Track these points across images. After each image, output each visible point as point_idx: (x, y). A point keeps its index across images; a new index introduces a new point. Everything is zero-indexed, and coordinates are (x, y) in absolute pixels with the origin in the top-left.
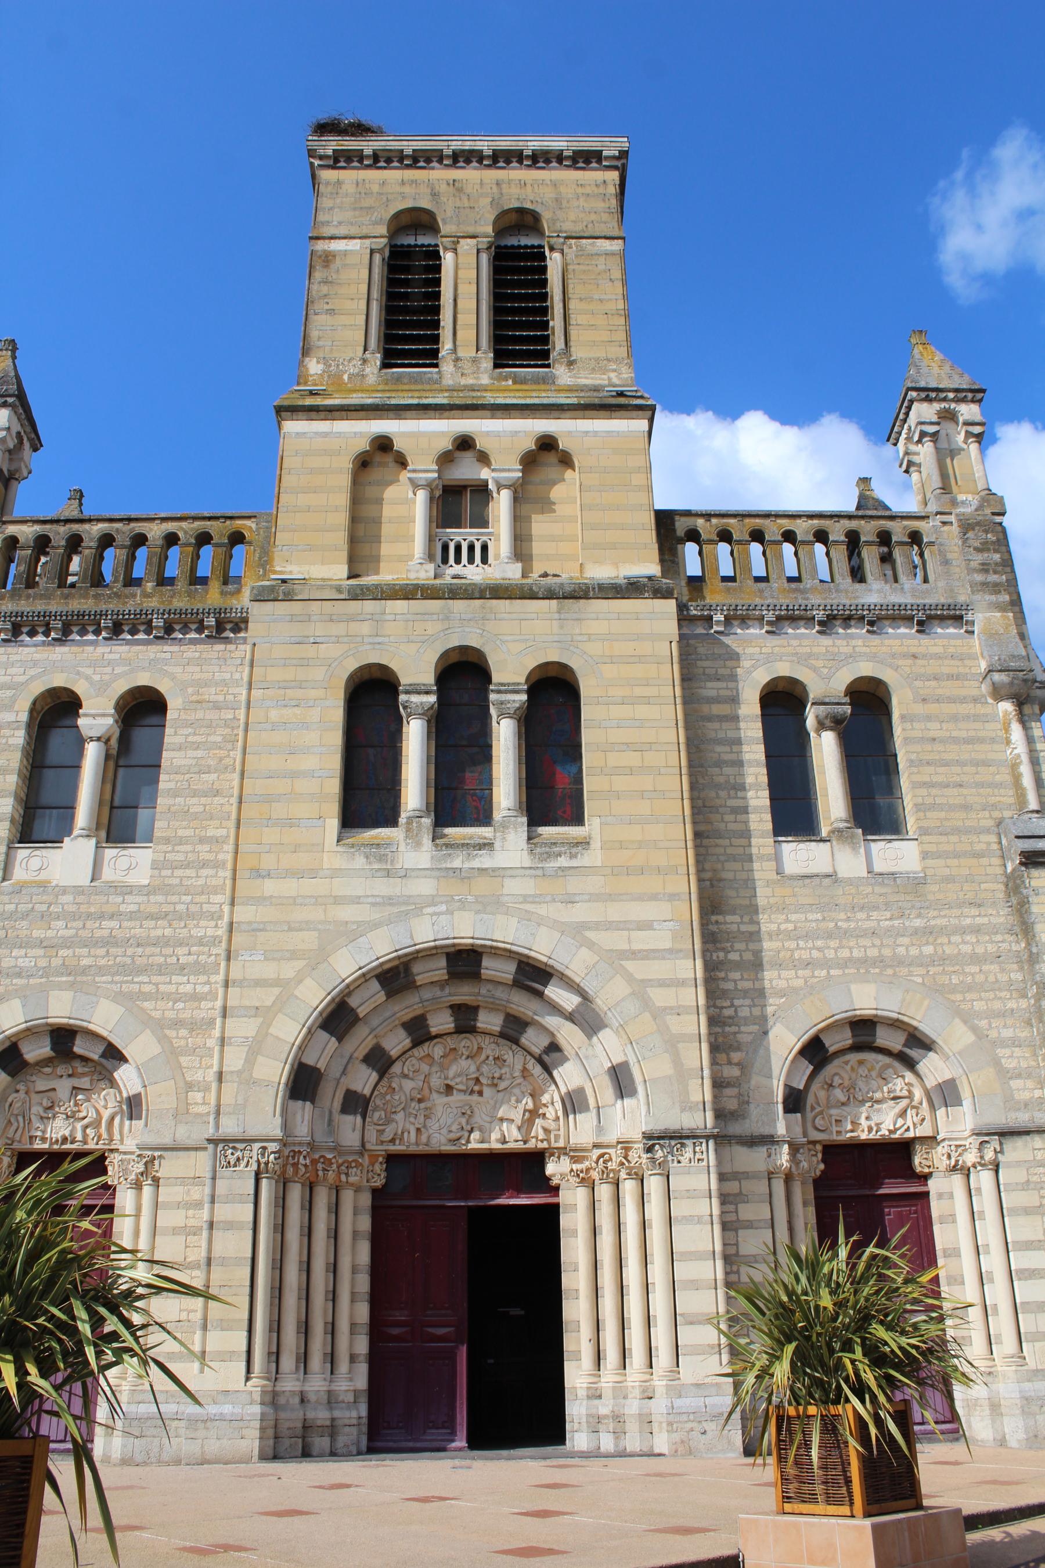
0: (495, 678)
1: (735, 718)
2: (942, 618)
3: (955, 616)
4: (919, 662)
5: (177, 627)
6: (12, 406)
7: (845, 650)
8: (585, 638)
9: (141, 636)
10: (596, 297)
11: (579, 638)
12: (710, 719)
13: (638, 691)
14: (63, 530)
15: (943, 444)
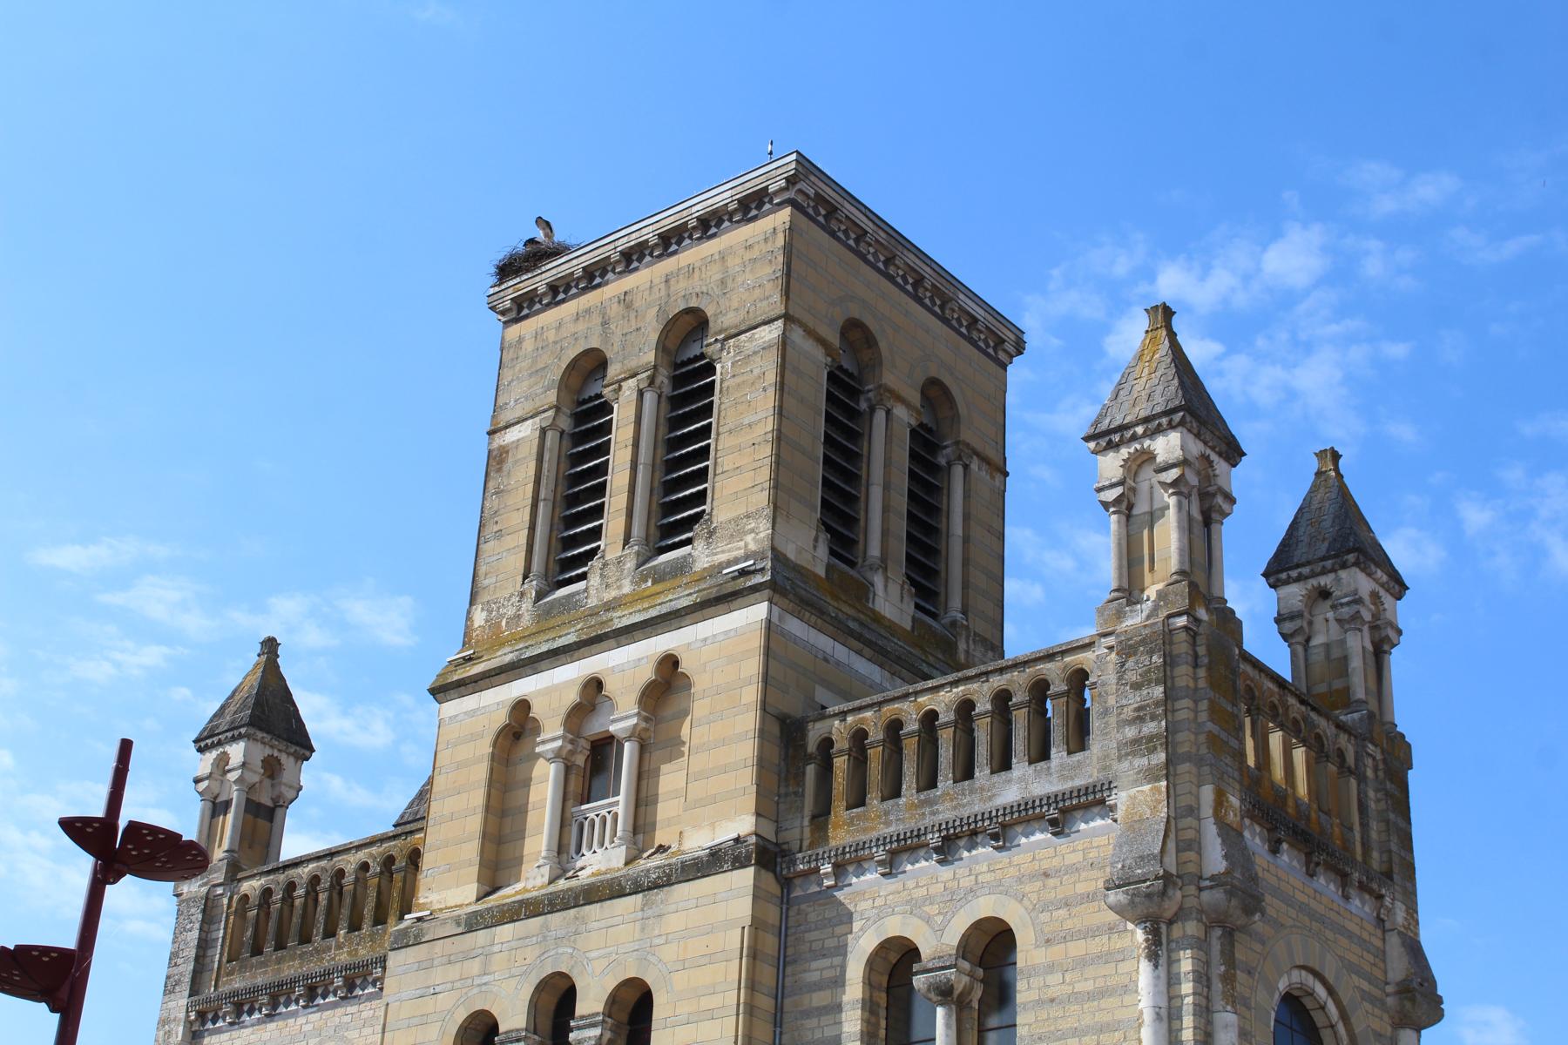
0: (581, 1008)
1: (838, 1008)
2: (1086, 807)
3: (1093, 800)
4: (1051, 882)
5: (358, 982)
6: (247, 736)
7: (967, 882)
8: (661, 941)
9: (331, 999)
10: (746, 422)
11: (657, 941)
12: (807, 1014)
13: (707, 1003)
14: (281, 877)
15: (1141, 508)
